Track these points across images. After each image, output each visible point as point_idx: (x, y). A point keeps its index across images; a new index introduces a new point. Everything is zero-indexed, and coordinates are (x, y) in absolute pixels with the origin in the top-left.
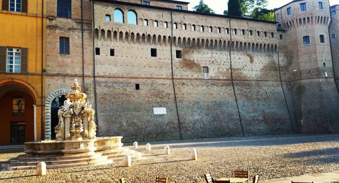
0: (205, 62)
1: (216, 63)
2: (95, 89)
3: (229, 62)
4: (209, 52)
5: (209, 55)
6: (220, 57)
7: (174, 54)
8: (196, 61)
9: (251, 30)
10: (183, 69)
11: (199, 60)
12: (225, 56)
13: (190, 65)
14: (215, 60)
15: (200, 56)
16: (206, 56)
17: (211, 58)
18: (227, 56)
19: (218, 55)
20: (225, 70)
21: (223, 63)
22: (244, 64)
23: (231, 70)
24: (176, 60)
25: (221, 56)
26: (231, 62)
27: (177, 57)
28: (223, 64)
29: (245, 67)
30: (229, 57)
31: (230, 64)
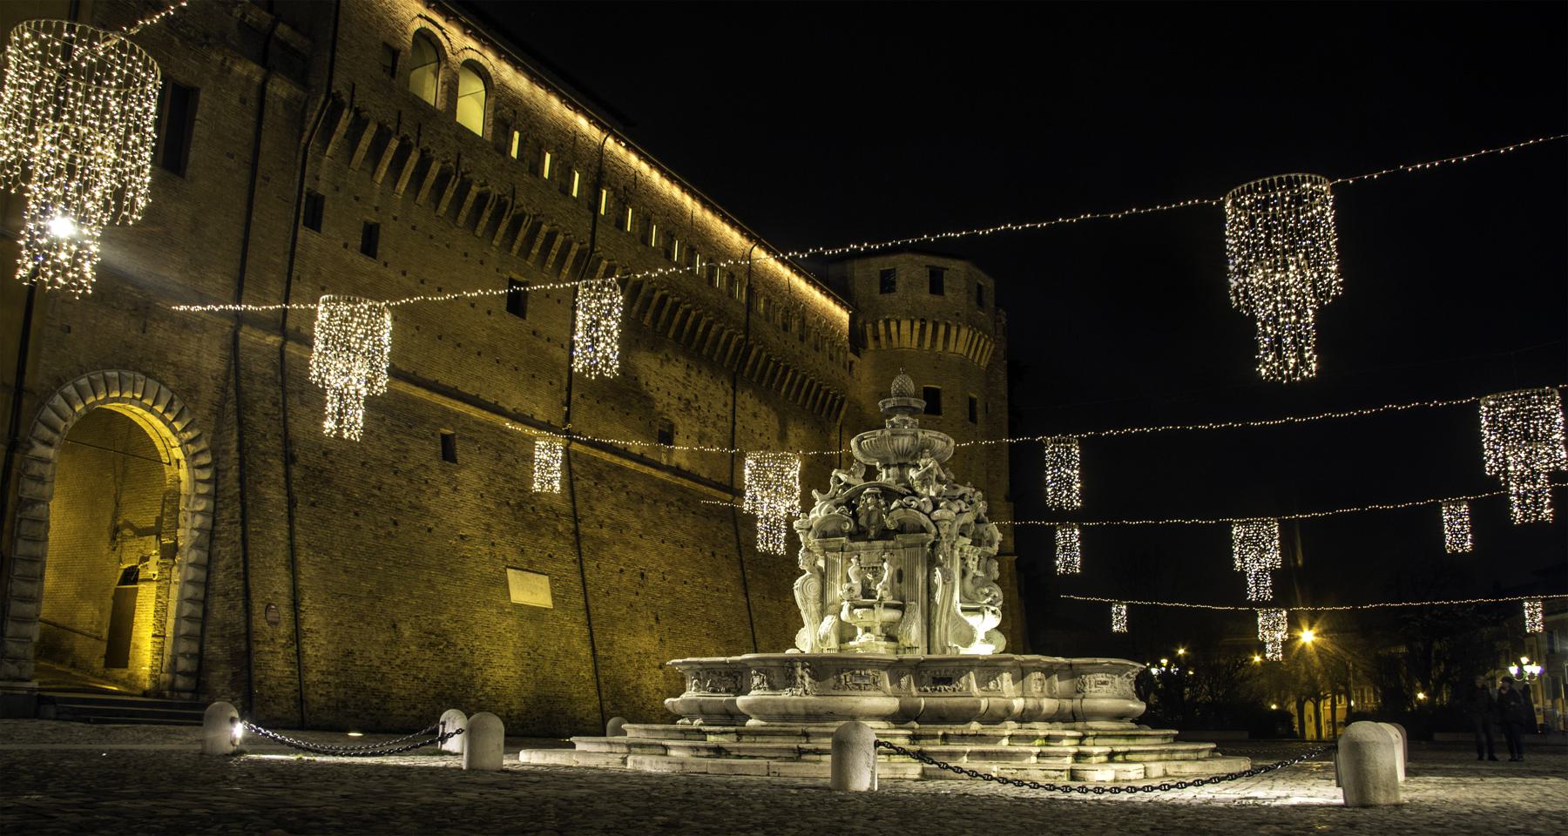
4: (681, 359)
5: (677, 371)
19: (702, 382)
26: (734, 423)
30: (729, 400)
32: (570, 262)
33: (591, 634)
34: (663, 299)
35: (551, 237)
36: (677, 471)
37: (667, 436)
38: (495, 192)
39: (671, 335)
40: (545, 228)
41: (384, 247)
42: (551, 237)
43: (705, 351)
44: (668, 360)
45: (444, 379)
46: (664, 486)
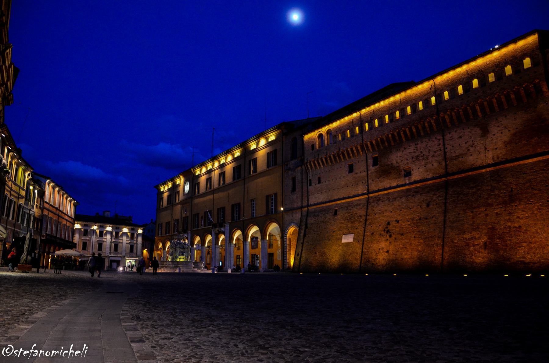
0: (406, 162)
1: (422, 156)
2: (307, 219)
3: (442, 149)
4: (412, 144)
5: (411, 149)
6: (428, 146)
7: (370, 162)
8: (395, 164)
9: (36, 240)
10: (380, 179)
11: (399, 161)
12: (436, 142)
13: (387, 171)
14: (420, 153)
15: (399, 154)
16: (408, 151)
17: (414, 152)
18: (439, 140)
20: (436, 165)
21: (432, 153)
22: (470, 143)
23: (446, 162)
24: (372, 169)
25: (430, 143)
26: (445, 149)
27: (374, 165)
28: (433, 156)
29: (470, 148)
30: (441, 141)
31: (443, 153)
32: (360, 150)
33: (363, 247)
34: (393, 135)
35: (352, 150)
36: (415, 182)
37: (408, 174)
38: (336, 152)
39: (404, 140)
40: (349, 149)
41: (322, 180)
42: (352, 150)
43: (422, 134)
44: (405, 148)
45: (336, 198)
46: (408, 190)
